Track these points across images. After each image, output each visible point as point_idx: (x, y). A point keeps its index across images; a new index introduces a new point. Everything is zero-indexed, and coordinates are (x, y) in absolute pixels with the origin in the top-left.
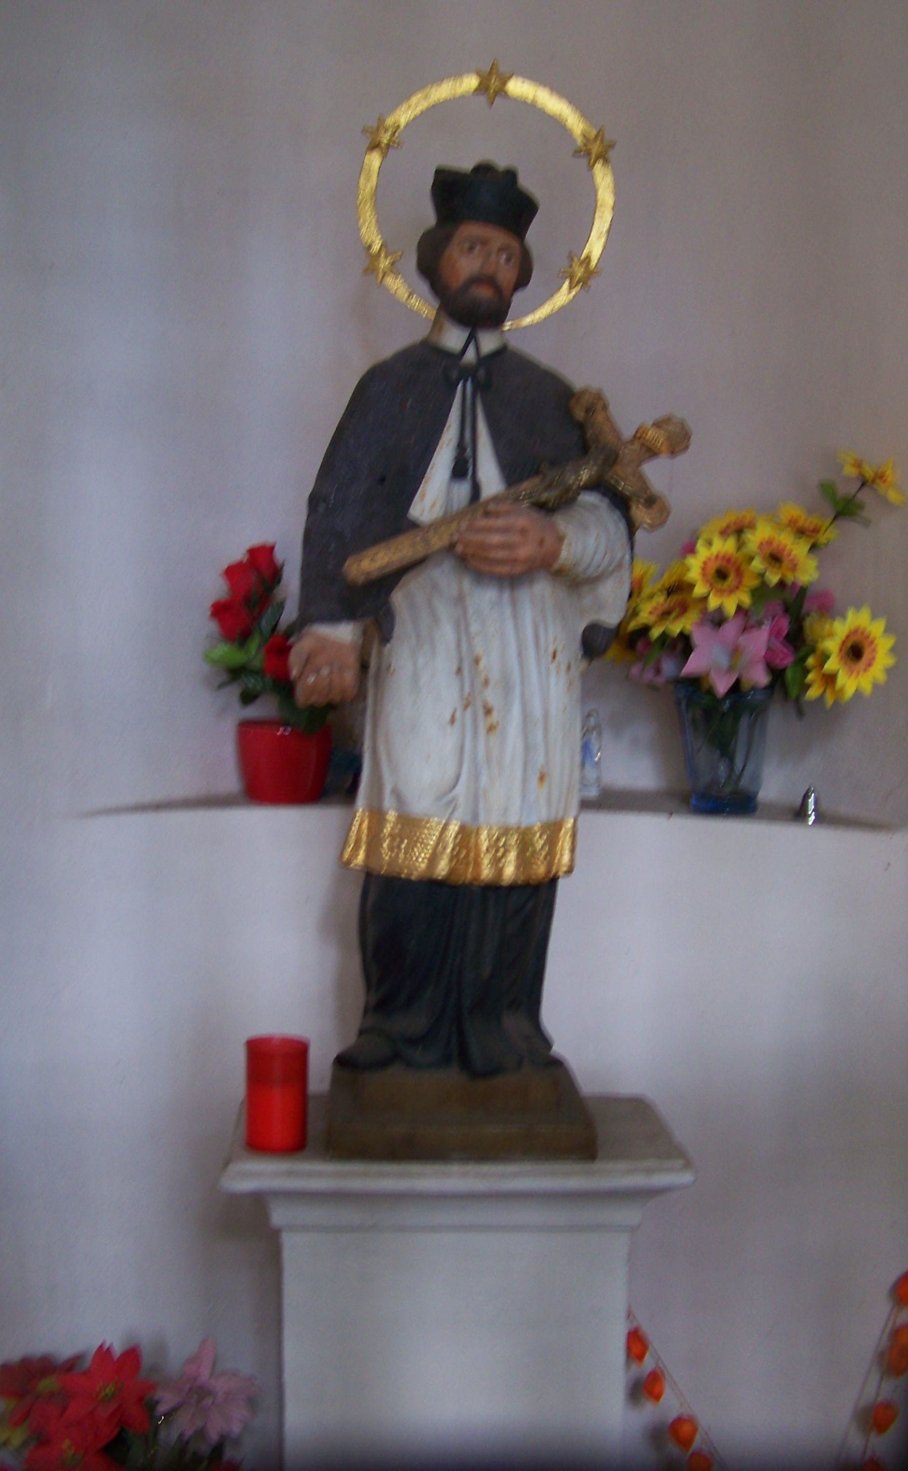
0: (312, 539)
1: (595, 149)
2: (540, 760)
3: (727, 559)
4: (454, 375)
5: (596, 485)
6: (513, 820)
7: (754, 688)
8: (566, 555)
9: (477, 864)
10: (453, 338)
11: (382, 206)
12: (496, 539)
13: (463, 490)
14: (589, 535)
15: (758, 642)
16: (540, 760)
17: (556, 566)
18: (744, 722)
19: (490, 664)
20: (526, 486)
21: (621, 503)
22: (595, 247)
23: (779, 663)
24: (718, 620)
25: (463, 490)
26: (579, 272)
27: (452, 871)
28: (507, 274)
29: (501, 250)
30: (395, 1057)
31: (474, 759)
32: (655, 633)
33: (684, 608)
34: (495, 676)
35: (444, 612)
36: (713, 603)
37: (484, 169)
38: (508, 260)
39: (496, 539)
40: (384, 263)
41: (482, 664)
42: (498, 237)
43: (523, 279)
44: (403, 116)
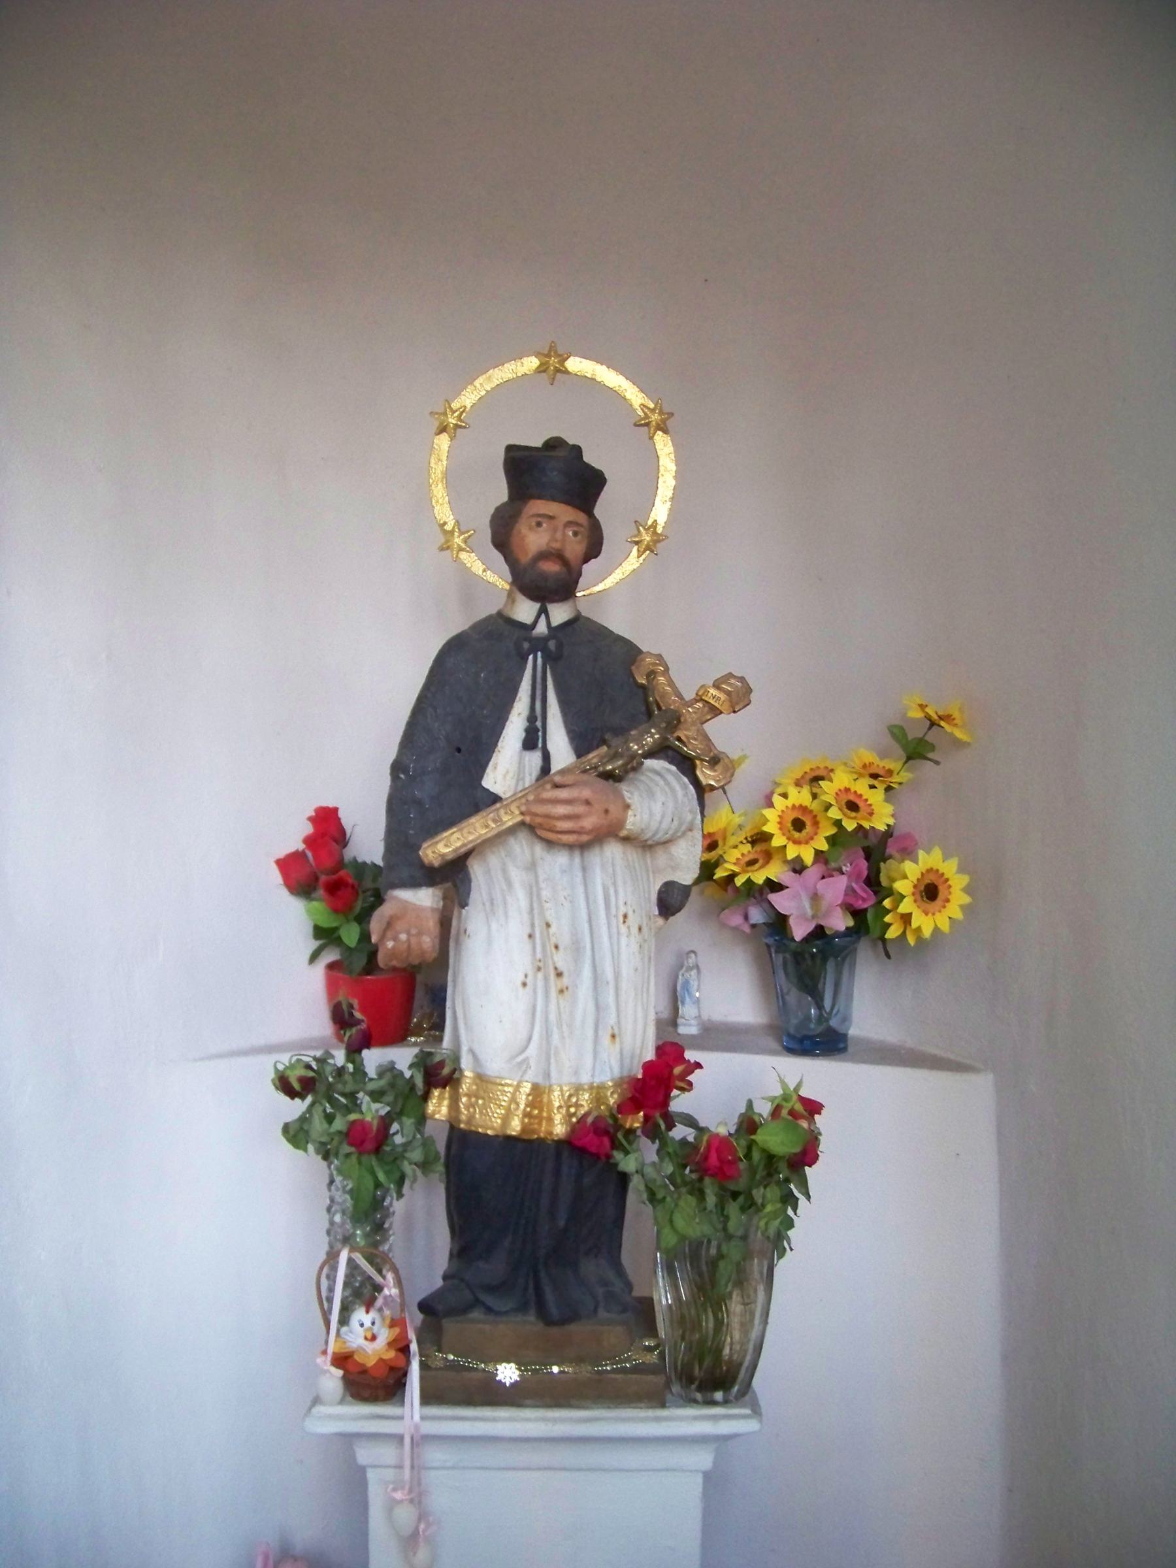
0: (396, 805)
1: (655, 417)
2: (612, 1019)
3: (803, 809)
4: (526, 645)
5: (662, 750)
6: (585, 1079)
7: (837, 934)
8: (633, 822)
9: (550, 1120)
10: (525, 611)
11: (453, 489)
12: (561, 810)
13: (535, 758)
14: (656, 798)
15: (835, 889)
16: (612, 1019)
17: (623, 833)
18: (830, 966)
19: (561, 931)
20: (593, 757)
21: (687, 765)
22: (660, 513)
23: (861, 905)
24: (798, 867)
25: (535, 758)
26: (647, 538)
27: (524, 1129)
28: (574, 547)
29: (569, 524)
30: (476, 1303)
31: (547, 1020)
32: (739, 881)
33: (768, 856)
34: (565, 940)
35: (517, 876)
36: (791, 853)
37: (554, 444)
38: (575, 534)
39: (561, 810)
40: (458, 540)
41: (553, 930)
42: (564, 512)
43: (594, 548)
44: (468, 399)
